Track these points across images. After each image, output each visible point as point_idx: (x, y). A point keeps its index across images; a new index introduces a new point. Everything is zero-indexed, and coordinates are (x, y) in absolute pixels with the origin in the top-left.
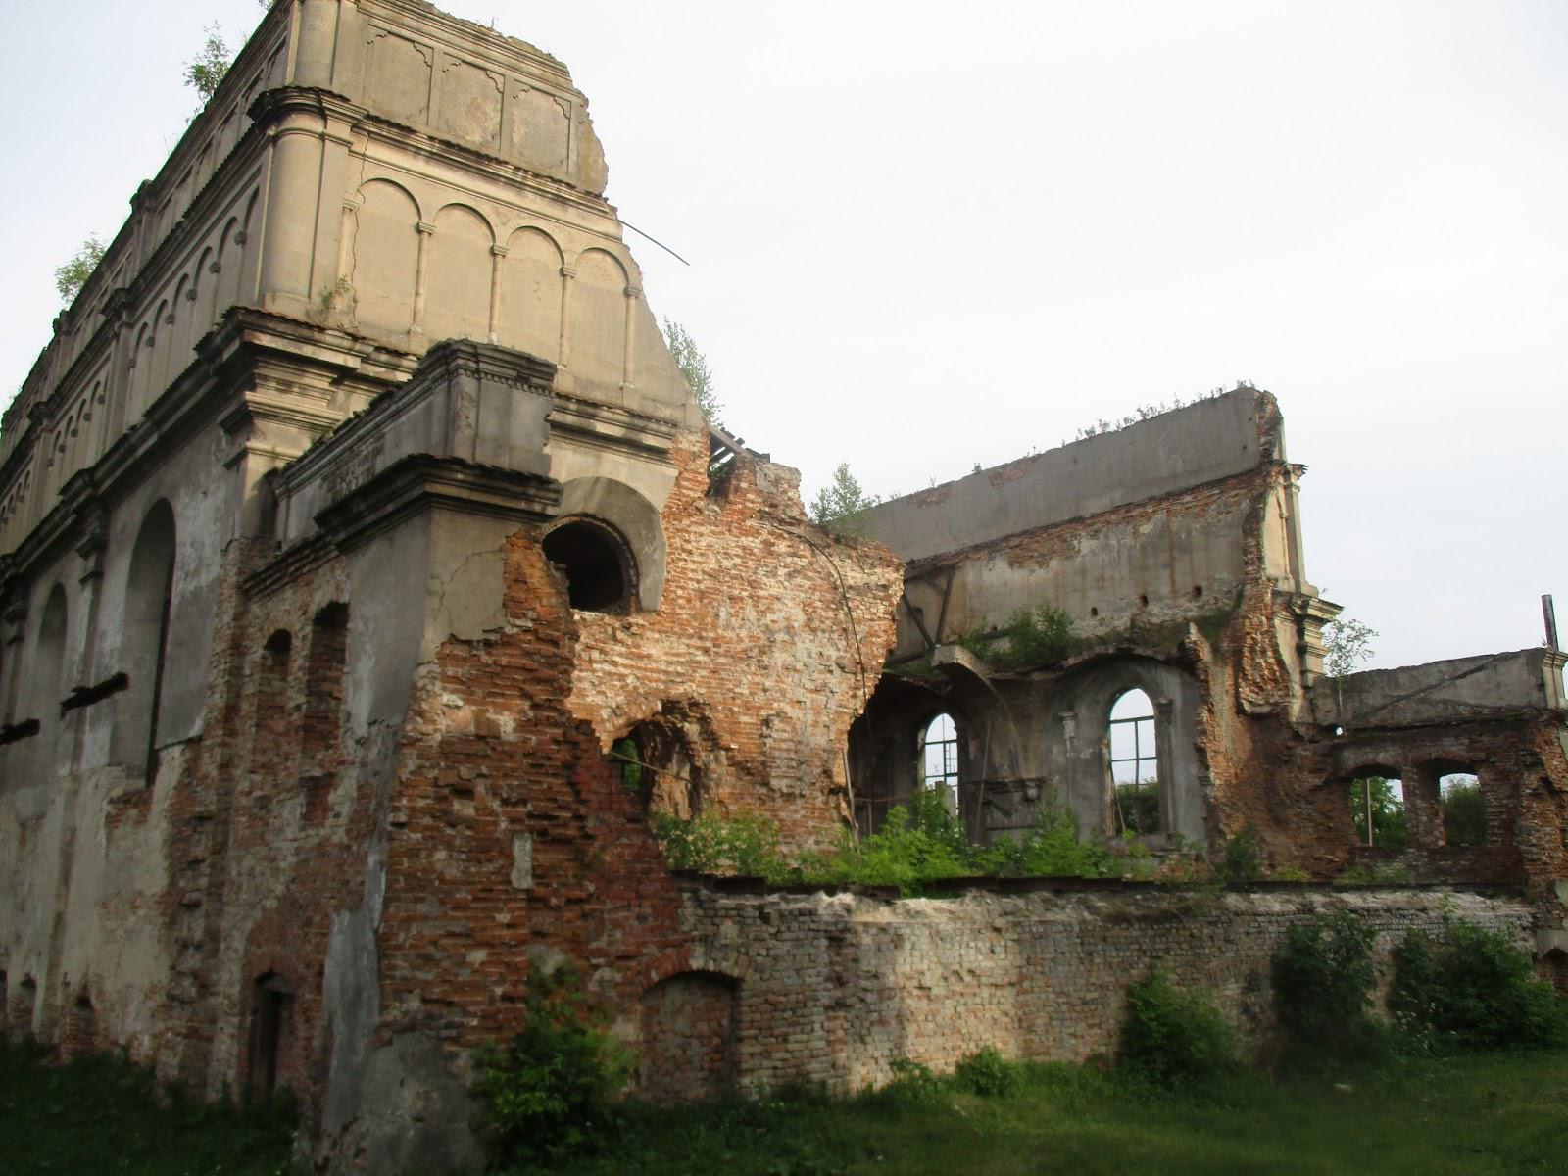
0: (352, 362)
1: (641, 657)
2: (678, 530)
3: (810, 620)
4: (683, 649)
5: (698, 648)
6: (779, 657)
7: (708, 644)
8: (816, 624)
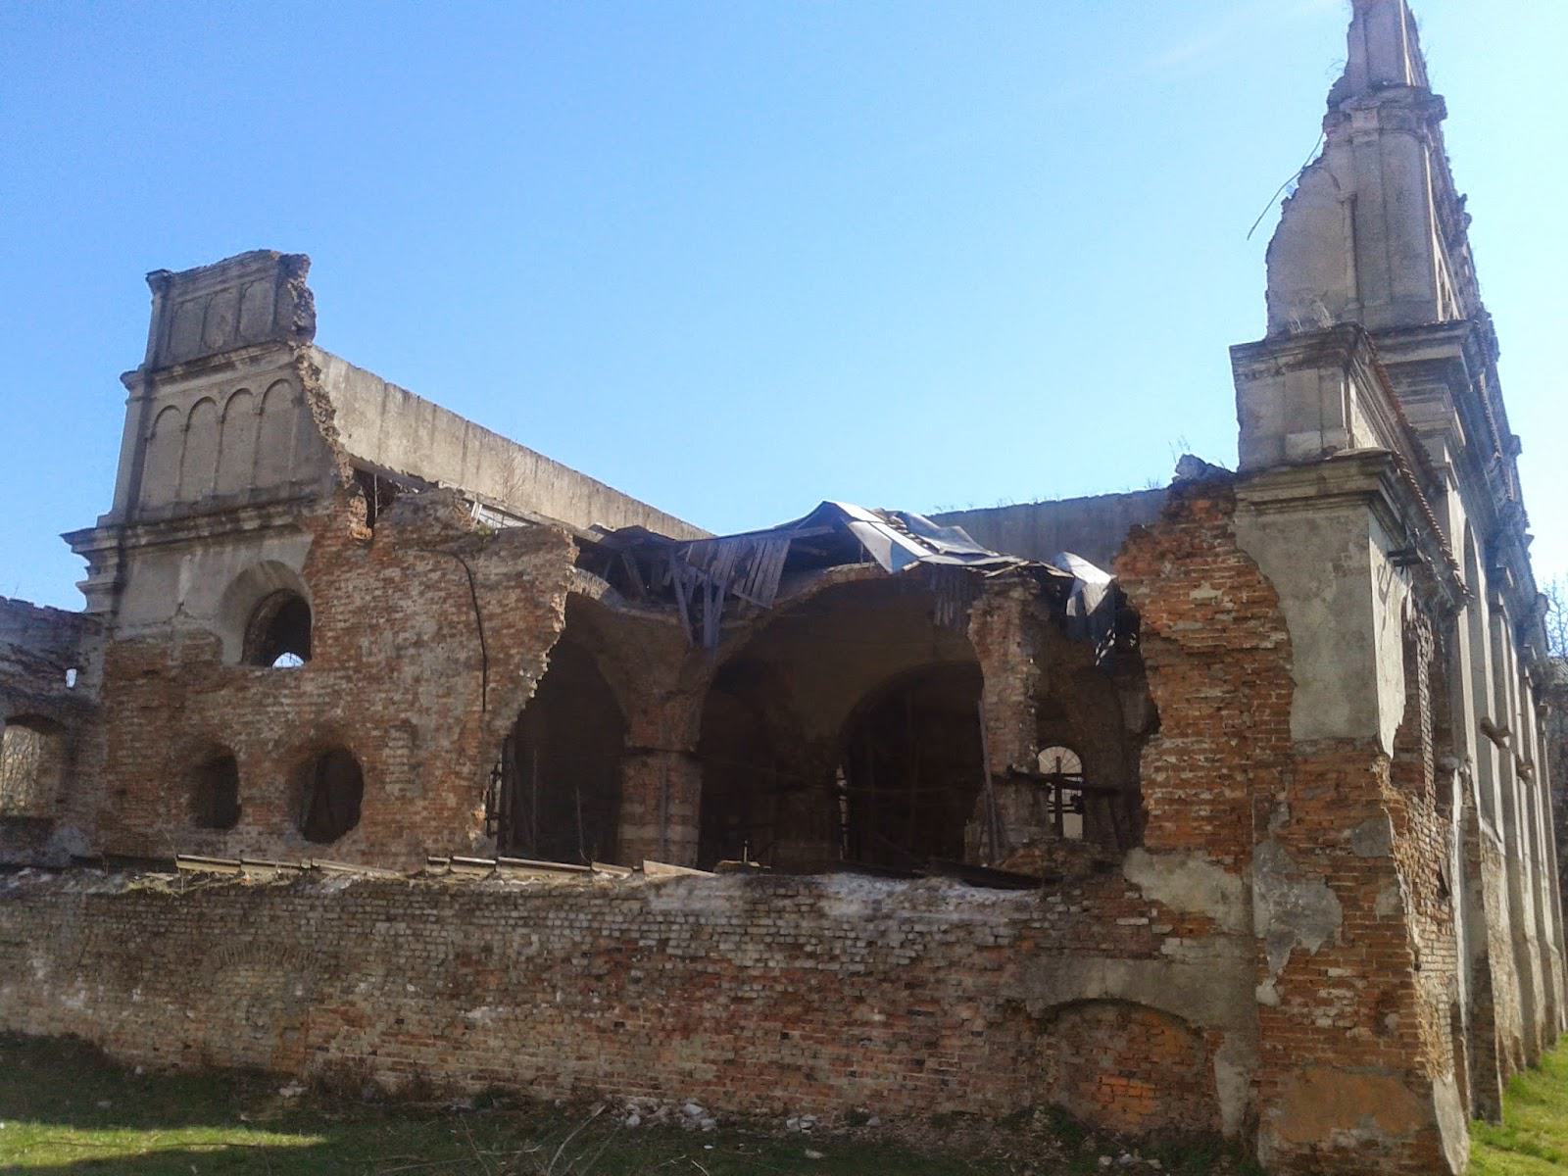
0: (114, 543)
1: (300, 696)
2: (333, 582)
3: (440, 628)
4: (332, 681)
5: (341, 678)
6: (408, 671)
7: (351, 672)
8: (445, 631)
